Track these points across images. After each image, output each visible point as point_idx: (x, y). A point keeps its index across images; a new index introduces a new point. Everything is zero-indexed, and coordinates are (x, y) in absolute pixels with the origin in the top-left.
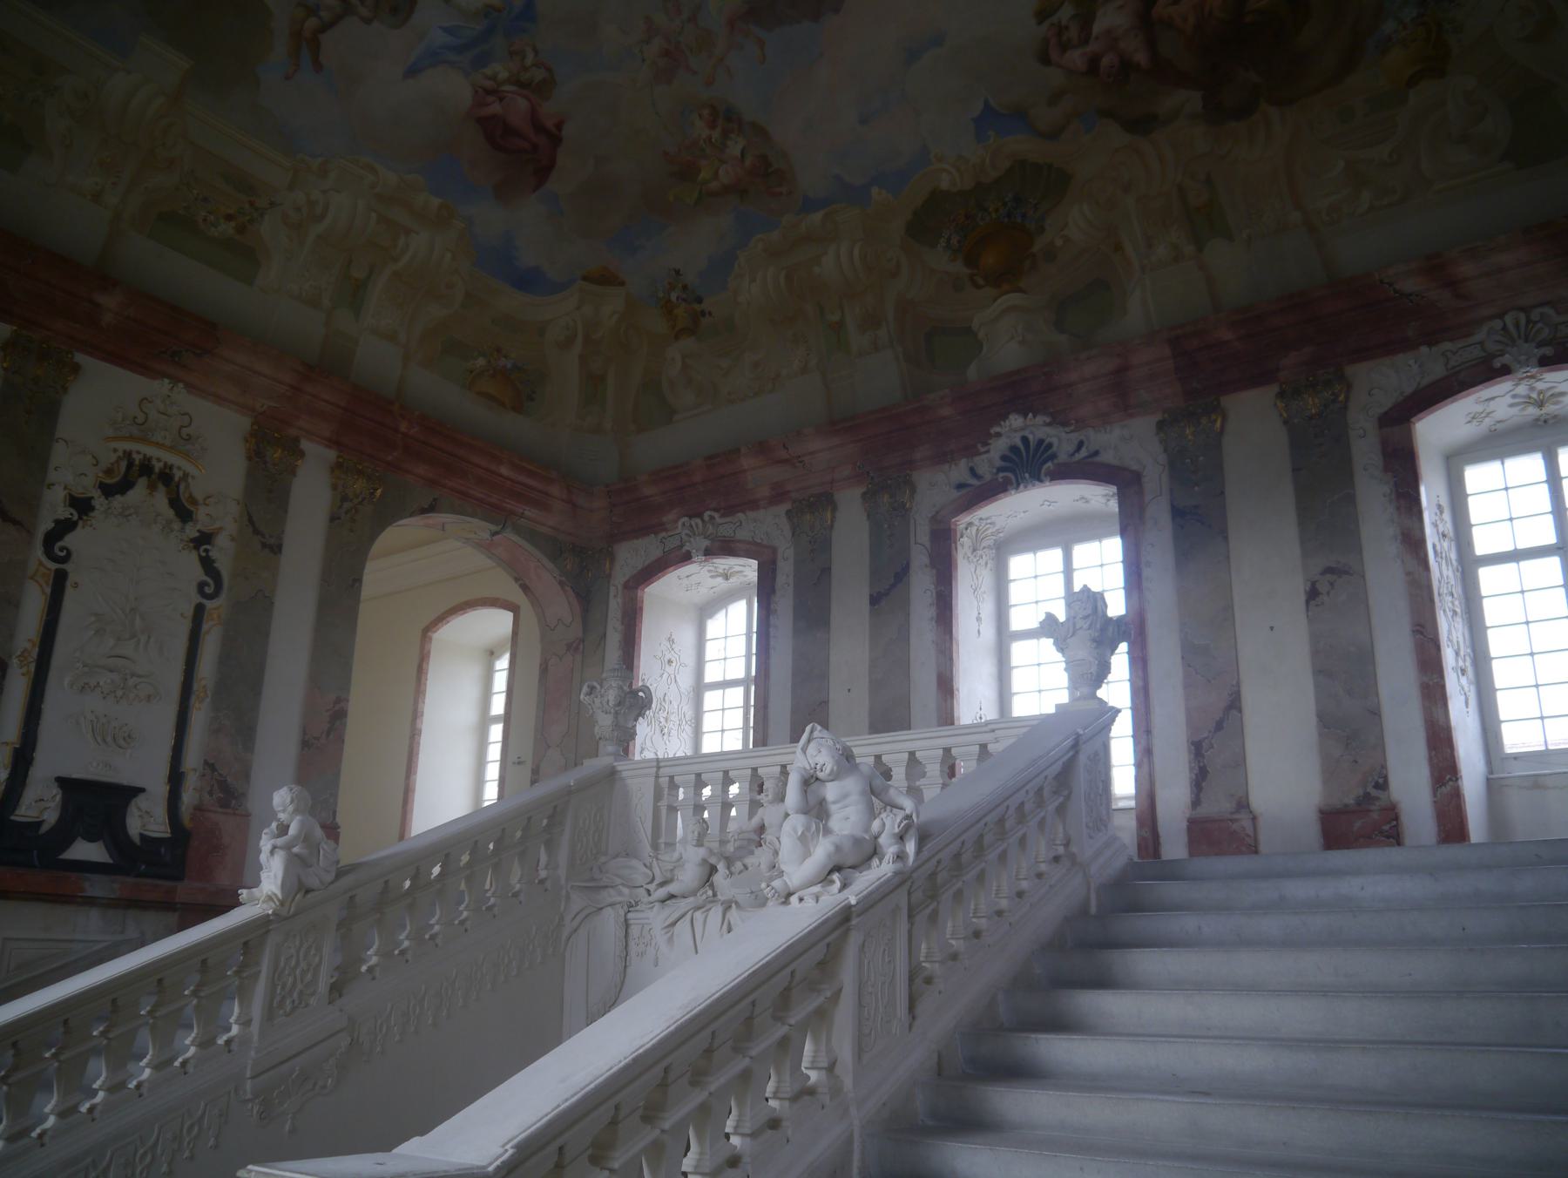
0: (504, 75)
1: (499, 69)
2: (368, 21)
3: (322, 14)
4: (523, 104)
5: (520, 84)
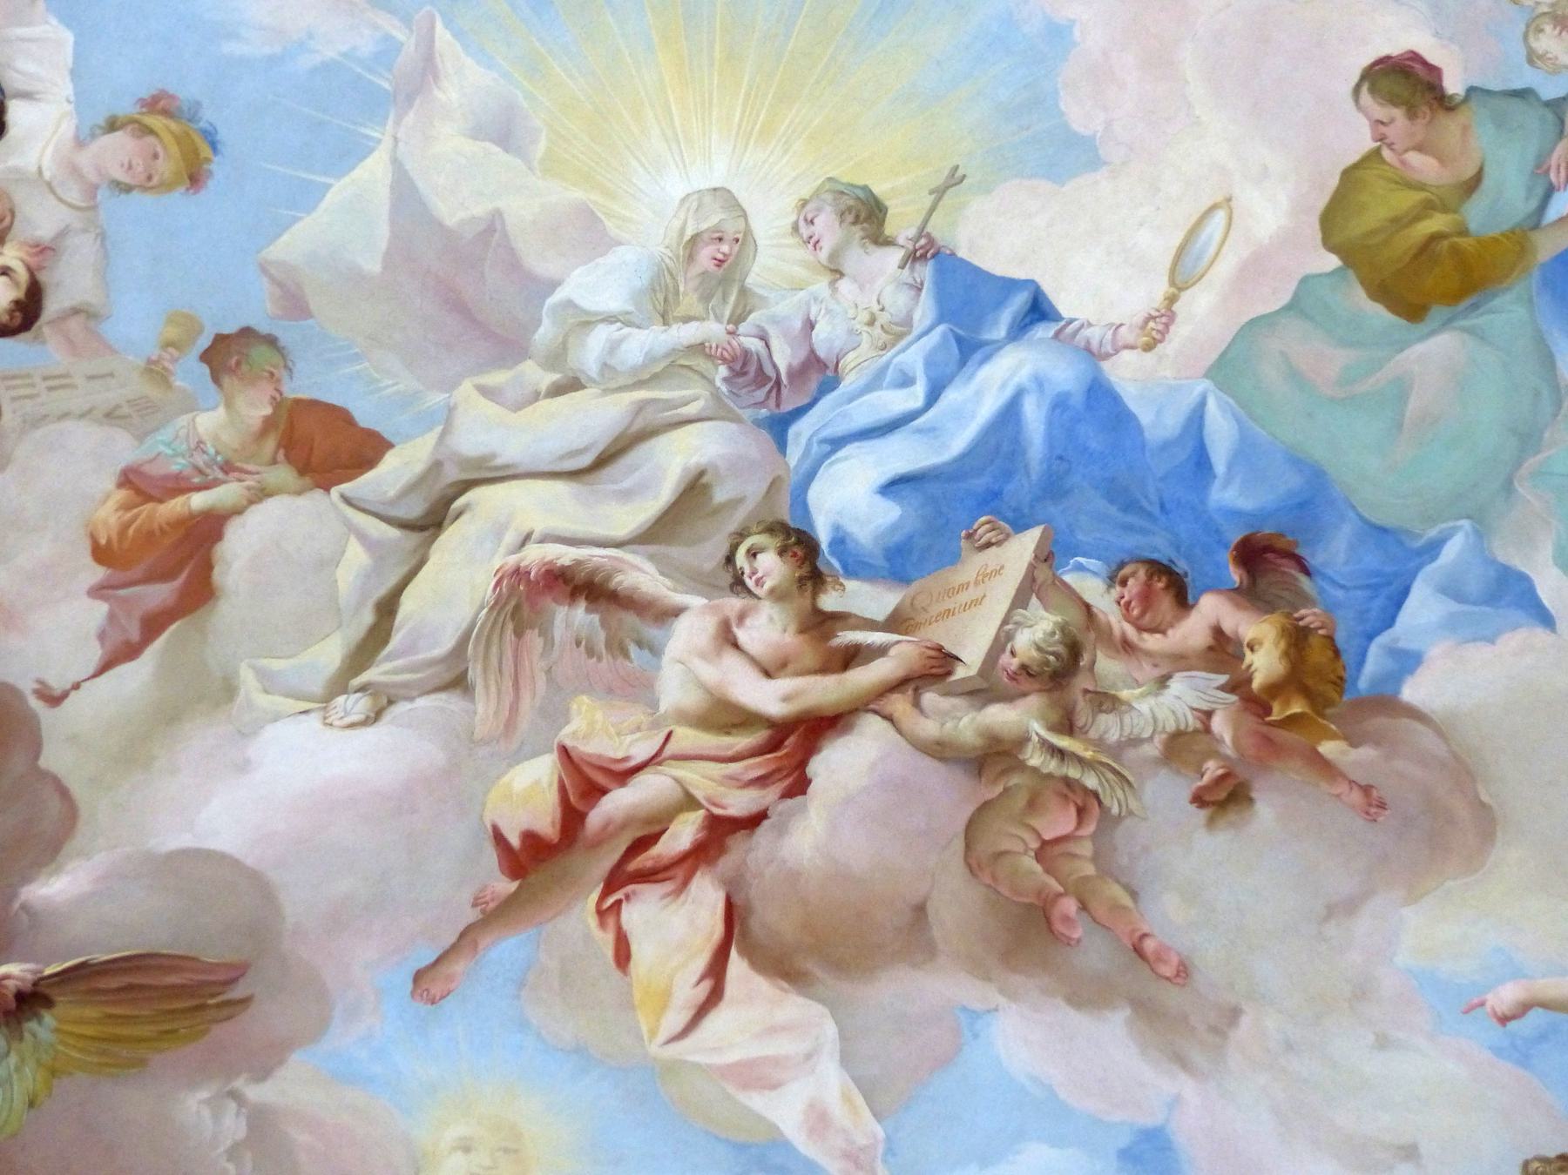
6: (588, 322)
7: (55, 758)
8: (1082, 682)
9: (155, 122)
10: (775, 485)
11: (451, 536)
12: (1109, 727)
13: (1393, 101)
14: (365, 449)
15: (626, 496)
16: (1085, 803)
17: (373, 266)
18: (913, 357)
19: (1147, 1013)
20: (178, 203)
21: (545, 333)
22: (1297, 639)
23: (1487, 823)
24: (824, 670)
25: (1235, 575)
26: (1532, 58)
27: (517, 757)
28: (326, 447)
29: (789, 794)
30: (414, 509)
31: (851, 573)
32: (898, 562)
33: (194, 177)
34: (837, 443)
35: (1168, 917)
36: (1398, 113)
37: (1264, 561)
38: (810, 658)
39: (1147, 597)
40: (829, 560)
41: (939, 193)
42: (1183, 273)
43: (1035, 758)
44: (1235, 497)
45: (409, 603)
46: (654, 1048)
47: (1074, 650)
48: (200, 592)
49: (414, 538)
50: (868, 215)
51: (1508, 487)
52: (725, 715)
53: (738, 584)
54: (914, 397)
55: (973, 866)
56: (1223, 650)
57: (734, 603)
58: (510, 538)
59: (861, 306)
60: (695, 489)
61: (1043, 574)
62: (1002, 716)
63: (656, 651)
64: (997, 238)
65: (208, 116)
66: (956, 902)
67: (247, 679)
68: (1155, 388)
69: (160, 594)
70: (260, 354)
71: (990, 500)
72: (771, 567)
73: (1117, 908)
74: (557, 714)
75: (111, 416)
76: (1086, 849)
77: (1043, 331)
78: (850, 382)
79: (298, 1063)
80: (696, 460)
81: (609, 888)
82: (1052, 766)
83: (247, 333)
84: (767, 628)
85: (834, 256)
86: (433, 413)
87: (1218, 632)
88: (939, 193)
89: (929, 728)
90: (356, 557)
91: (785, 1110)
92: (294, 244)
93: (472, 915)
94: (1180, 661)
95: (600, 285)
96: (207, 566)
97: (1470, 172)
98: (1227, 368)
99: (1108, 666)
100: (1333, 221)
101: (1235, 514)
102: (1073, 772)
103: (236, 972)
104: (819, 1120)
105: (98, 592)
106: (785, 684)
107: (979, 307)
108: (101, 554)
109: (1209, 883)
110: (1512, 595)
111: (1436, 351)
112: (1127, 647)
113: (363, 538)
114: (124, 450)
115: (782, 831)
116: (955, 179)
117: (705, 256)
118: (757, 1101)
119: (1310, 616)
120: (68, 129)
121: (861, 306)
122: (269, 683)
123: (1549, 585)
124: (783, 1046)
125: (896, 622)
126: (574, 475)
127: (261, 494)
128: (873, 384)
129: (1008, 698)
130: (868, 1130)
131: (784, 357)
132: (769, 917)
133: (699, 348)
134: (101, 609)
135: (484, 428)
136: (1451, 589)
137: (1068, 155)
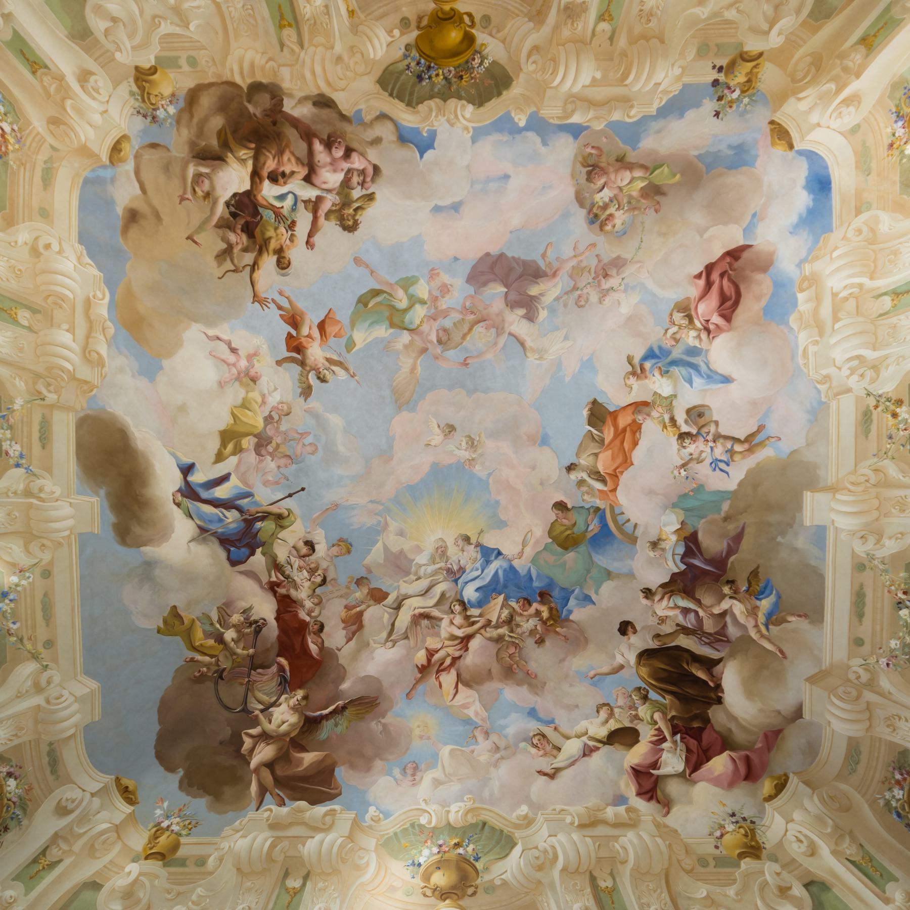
0: (693, 333)
1: (690, 338)
4: (702, 308)
5: (690, 318)
79: (389, 714)
81: (437, 673)
91: (470, 712)
103: (377, 698)
104: (477, 714)
118: (466, 711)
124: (471, 700)
130: (484, 714)
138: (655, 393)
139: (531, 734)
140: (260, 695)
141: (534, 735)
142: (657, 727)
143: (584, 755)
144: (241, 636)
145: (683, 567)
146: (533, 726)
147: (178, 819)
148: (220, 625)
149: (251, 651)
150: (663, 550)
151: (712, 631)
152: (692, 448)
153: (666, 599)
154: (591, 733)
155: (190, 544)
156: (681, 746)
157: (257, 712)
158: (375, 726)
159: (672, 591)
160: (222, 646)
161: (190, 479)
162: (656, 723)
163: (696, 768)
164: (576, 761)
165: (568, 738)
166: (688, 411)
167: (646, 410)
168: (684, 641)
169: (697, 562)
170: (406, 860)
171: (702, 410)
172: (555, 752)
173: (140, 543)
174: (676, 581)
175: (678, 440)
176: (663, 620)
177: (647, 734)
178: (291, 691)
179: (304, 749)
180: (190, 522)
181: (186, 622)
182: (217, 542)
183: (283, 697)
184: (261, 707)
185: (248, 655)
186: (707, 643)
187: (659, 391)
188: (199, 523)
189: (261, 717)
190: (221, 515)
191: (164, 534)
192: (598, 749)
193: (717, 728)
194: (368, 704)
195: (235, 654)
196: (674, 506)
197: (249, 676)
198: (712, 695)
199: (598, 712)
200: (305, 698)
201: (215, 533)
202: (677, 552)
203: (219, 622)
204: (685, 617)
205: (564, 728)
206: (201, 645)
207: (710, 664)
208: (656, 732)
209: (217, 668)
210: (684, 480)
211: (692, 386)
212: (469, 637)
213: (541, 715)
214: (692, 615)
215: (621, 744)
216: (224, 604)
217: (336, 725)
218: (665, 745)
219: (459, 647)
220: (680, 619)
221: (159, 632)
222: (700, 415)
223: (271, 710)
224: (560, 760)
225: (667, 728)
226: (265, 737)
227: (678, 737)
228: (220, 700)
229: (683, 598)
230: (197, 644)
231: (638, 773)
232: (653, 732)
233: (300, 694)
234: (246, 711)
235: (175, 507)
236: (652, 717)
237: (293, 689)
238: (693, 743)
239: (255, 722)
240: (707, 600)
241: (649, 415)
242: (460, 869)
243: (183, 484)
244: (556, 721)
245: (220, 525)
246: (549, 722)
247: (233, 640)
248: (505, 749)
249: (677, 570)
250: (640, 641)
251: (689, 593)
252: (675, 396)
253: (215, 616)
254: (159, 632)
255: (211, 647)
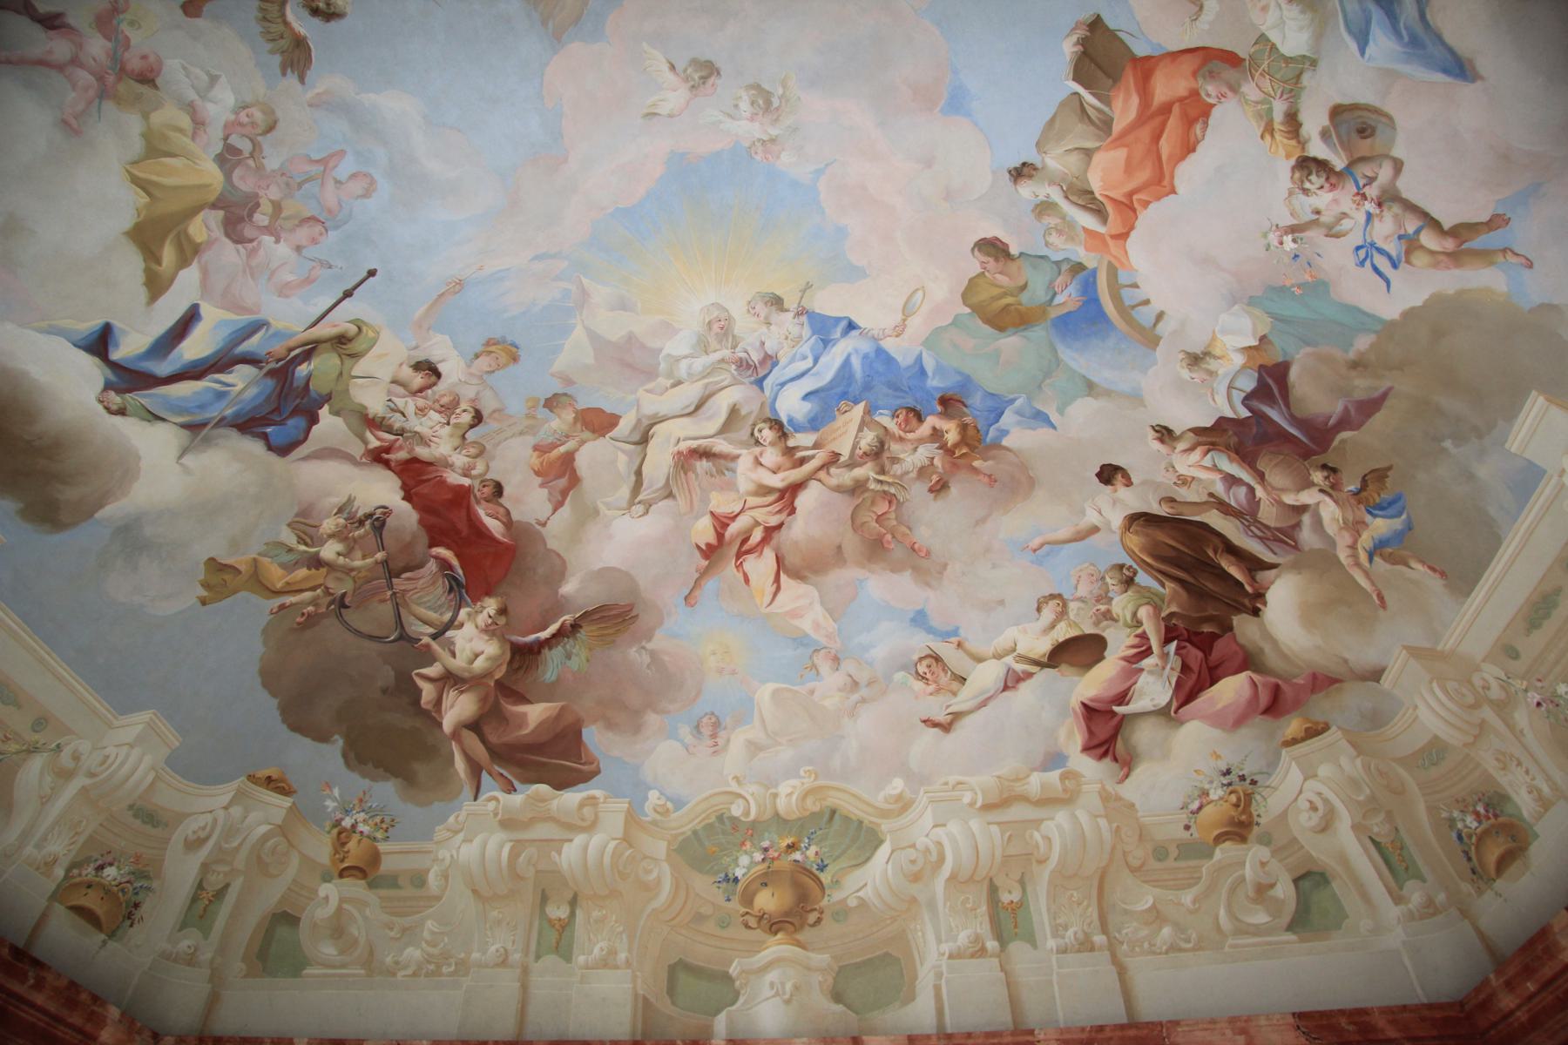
2: (1398, 166)
3: (1411, 230)
6: (678, 360)
7: (552, 544)
8: (886, 454)
9: (492, 348)
10: (762, 404)
11: (652, 443)
12: (897, 469)
13: (989, 255)
14: (611, 421)
15: (710, 418)
16: (891, 499)
17: (590, 360)
18: (806, 349)
19: (916, 570)
20: (513, 368)
21: (663, 366)
22: (964, 428)
23: (1032, 483)
24: (794, 467)
25: (939, 408)
26: (1047, 244)
27: (697, 518)
28: (599, 423)
29: (789, 514)
30: (636, 437)
31: (797, 431)
32: (814, 424)
33: (515, 359)
34: (783, 384)
35: (923, 535)
36: (991, 260)
37: (948, 404)
38: (788, 464)
39: (907, 421)
40: (788, 428)
41: (804, 291)
42: (907, 311)
43: (872, 486)
44: (935, 383)
45: (644, 468)
46: (764, 610)
47: (882, 444)
48: (575, 480)
49: (639, 448)
50: (777, 302)
51: (1040, 387)
52: (764, 490)
53: (757, 443)
54: (809, 363)
55: (855, 530)
56: (936, 434)
57: (757, 450)
58: (673, 441)
59: (782, 335)
60: (734, 412)
61: (867, 419)
62: (859, 472)
63: (734, 471)
64: (828, 303)
65: (509, 338)
66: (851, 542)
67: (602, 508)
68: (902, 350)
69: (562, 482)
70: (564, 399)
71: (844, 395)
72: (768, 434)
73: (904, 535)
74: (705, 500)
75: (521, 433)
76: (893, 516)
77: (854, 333)
78: (783, 361)
79: (659, 635)
80: (731, 401)
82: (879, 487)
83: (555, 395)
84: (771, 456)
85: (766, 318)
86: (632, 403)
87: (934, 429)
88: (804, 291)
89: (834, 482)
90: (622, 459)
91: (806, 625)
92: (561, 363)
93: (696, 575)
94: (921, 441)
95: (678, 346)
96: (574, 471)
97: (1022, 283)
98: (930, 342)
99: (895, 447)
100: (966, 297)
101: (937, 389)
102: (886, 488)
103: (631, 607)
104: (817, 626)
105: (542, 485)
106: (781, 475)
107: (825, 329)
108: (538, 473)
109: (936, 521)
110: (1041, 418)
111: (1010, 342)
112: (901, 439)
113: (623, 451)
114: (531, 440)
115: (790, 528)
116: (808, 286)
117: (716, 327)
118: (797, 622)
119: (968, 420)
120: (462, 364)
121: (782, 335)
122: (609, 506)
123: (1054, 417)
125: (816, 446)
126: (689, 414)
127: (583, 443)
128: (792, 360)
129: (860, 465)
130: (831, 625)
131: (756, 357)
132: (791, 559)
133: (722, 361)
134: (546, 491)
135: (652, 404)
136: (1018, 413)
137: (855, 274)
138: (1262, 39)
139: (916, 657)
140: (422, 611)
141: (921, 659)
142: (1139, 631)
143: (1006, 688)
144: (351, 546)
145: (1244, 413)
146: (920, 642)
147: (362, 816)
148: (306, 544)
149: (380, 556)
150: (1211, 373)
151: (1272, 524)
152: (1323, 199)
153: (1199, 451)
154: (1021, 650)
155: (183, 461)
156: (1175, 662)
157: (426, 640)
158: (635, 655)
159: (1213, 444)
160: (323, 570)
161: (115, 355)
162: (1139, 623)
163: (1190, 697)
164: (989, 699)
165: (979, 659)
166: (1337, 112)
167: (1230, 74)
168: (1215, 520)
169: (1274, 414)
170: (716, 873)
171: (1371, 119)
172: (955, 685)
173: (86, 511)
174: (1225, 431)
175: (1293, 169)
176: (1184, 481)
177: (1119, 643)
178: (475, 601)
179: (523, 699)
180: (160, 426)
181: (242, 568)
182: (234, 433)
183: (463, 612)
184: (431, 630)
185: (377, 562)
186: (1256, 536)
187: (1274, 36)
188: (180, 420)
189: (435, 645)
190: (217, 386)
191: (125, 468)
192: (1030, 675)
193: (1241, 640)
194: (615, 618)
195: (352, 570)
196: (1252, 302)
197: (391, 586)
198: (1246, 602)
199: (1039, 610)
200: (503, 611)
201: (221, 420)
202: (1239, 383)
203: (301, 541)
204: (1228, 489)
205: (974, 645)
206: (288, 583)
207: (1254, 565)
208: (1137, 641)
209: (330, 598)
210: (1287, 260)
211: (1362, 52)
212: (795, 488)
213: (935, 622)
214: (1242, 491)
215: (1072, 665)
216: (297, 515)
217: (569, 657)
218: (1147, 662)
219: (777, 507)
220: (1219, 488)
221: (204, 602)
222: (1365, 131)
223: (449, 634)
224: (964, 698)
225: (1158, 631)
226: (450, 679)
227: (1174, 645)
228: (358, 633)
229: (1231, 460)
230: (279, 585)
231: (1091, 712)
232: (1133, 641)
233: (491, 605)
234: (404, 637)
235: (118, 420)
236: (1134, 614)
237: (475, 600)
238: (1195, 655)
239: (430, 659)
240: (1276, 478)
241: (1234, 89)
242: (797, 885)
243: (109, 372)
244: (961, 632)
245: (223, 403)
246: (945, 636)
247: (339, 554)
248: (869, 684)
249: (1230, 414)
250: (1131, 500)
251: (1246, 456)
252: (1314, 63)
253: (289, 538)
254: (204, 602)
255: (306, 579)
